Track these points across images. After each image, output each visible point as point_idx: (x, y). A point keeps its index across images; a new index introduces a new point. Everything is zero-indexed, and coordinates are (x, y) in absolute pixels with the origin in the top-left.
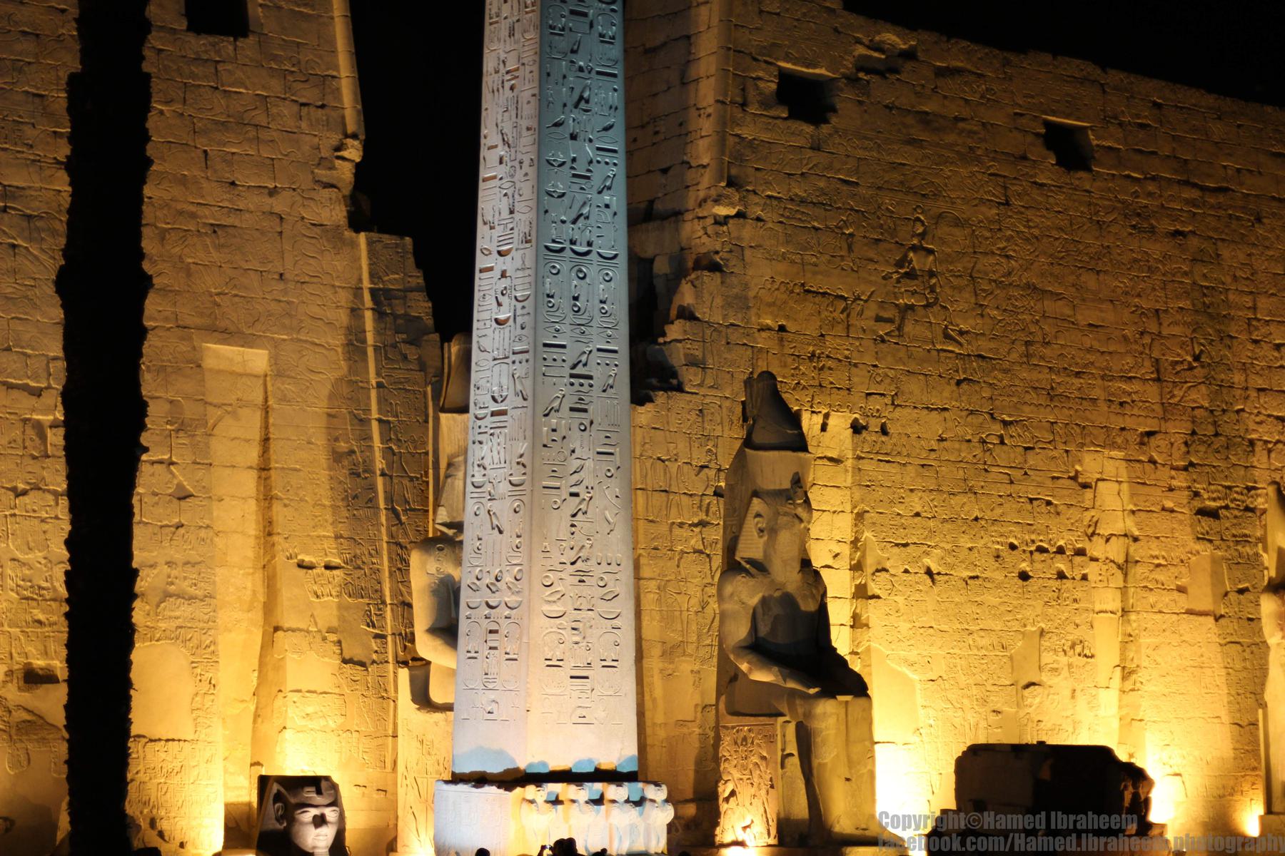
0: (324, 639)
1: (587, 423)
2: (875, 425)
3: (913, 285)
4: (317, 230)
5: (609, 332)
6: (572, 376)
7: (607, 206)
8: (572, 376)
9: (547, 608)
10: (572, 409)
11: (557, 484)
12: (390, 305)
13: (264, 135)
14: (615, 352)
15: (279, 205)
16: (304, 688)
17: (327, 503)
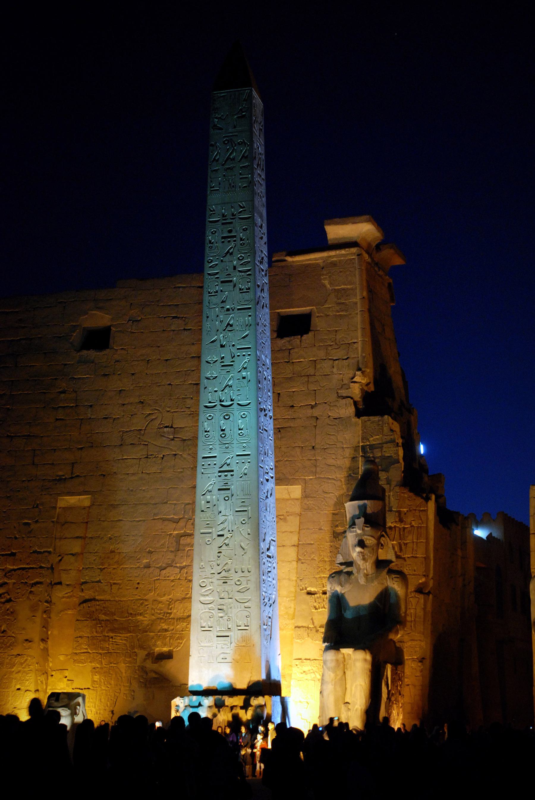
0: (317, 631)
1: (230, 496)
4: (337, 421)
5: (244, 445)
6: (220, 472)
7: (244, 378)
8: (220, 472)
9: (202, 599)
10: (219, 490)
11: (210, 531)
12: (372, 452)
13: (312, 379)
14: (249, 455)
15: (316, 412)
16: (303, 658)
17: (326, 559)
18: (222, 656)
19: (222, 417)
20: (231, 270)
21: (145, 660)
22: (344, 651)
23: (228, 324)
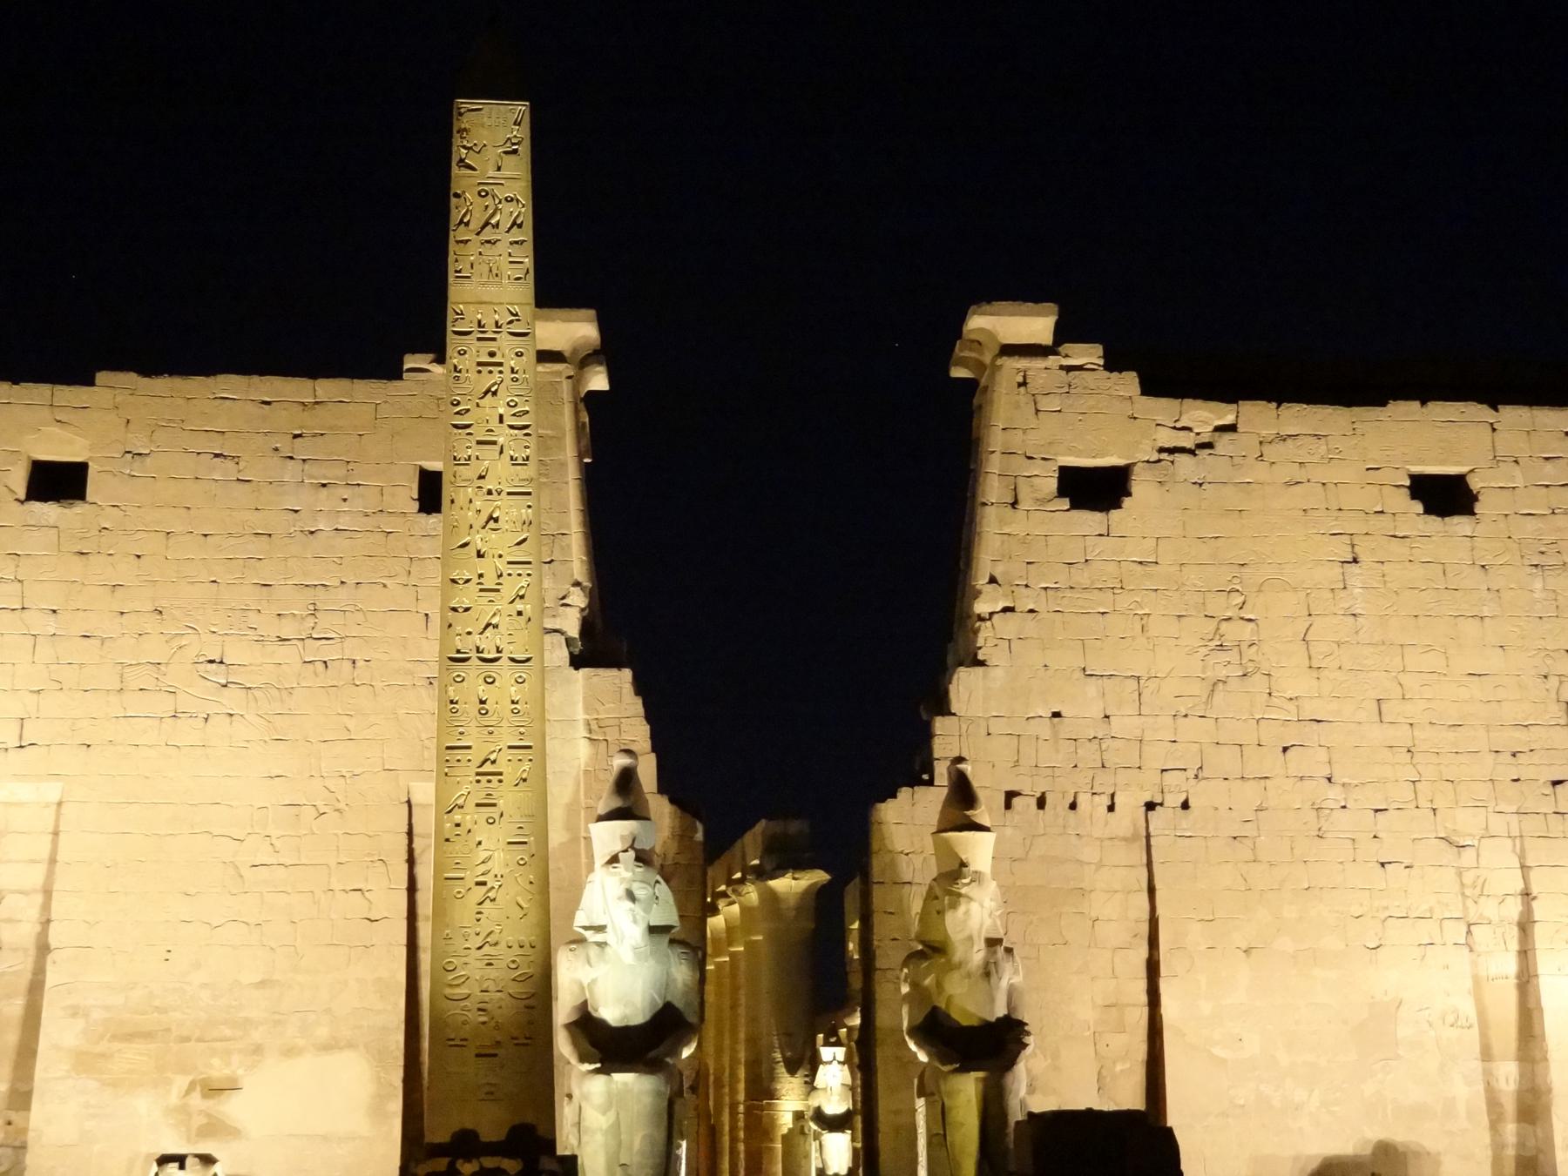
2: (1173, 800)
3: (1223, 657)
7: (520, 613)
10: (478, 805)
18: (487, 1089)
19: (481, 680)
20: (494, 423)
21: (188, 1092)
22: (617, 1077)
23: (491, 518)
